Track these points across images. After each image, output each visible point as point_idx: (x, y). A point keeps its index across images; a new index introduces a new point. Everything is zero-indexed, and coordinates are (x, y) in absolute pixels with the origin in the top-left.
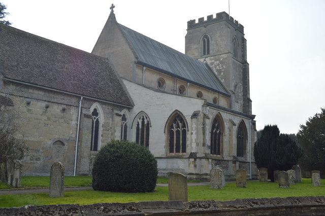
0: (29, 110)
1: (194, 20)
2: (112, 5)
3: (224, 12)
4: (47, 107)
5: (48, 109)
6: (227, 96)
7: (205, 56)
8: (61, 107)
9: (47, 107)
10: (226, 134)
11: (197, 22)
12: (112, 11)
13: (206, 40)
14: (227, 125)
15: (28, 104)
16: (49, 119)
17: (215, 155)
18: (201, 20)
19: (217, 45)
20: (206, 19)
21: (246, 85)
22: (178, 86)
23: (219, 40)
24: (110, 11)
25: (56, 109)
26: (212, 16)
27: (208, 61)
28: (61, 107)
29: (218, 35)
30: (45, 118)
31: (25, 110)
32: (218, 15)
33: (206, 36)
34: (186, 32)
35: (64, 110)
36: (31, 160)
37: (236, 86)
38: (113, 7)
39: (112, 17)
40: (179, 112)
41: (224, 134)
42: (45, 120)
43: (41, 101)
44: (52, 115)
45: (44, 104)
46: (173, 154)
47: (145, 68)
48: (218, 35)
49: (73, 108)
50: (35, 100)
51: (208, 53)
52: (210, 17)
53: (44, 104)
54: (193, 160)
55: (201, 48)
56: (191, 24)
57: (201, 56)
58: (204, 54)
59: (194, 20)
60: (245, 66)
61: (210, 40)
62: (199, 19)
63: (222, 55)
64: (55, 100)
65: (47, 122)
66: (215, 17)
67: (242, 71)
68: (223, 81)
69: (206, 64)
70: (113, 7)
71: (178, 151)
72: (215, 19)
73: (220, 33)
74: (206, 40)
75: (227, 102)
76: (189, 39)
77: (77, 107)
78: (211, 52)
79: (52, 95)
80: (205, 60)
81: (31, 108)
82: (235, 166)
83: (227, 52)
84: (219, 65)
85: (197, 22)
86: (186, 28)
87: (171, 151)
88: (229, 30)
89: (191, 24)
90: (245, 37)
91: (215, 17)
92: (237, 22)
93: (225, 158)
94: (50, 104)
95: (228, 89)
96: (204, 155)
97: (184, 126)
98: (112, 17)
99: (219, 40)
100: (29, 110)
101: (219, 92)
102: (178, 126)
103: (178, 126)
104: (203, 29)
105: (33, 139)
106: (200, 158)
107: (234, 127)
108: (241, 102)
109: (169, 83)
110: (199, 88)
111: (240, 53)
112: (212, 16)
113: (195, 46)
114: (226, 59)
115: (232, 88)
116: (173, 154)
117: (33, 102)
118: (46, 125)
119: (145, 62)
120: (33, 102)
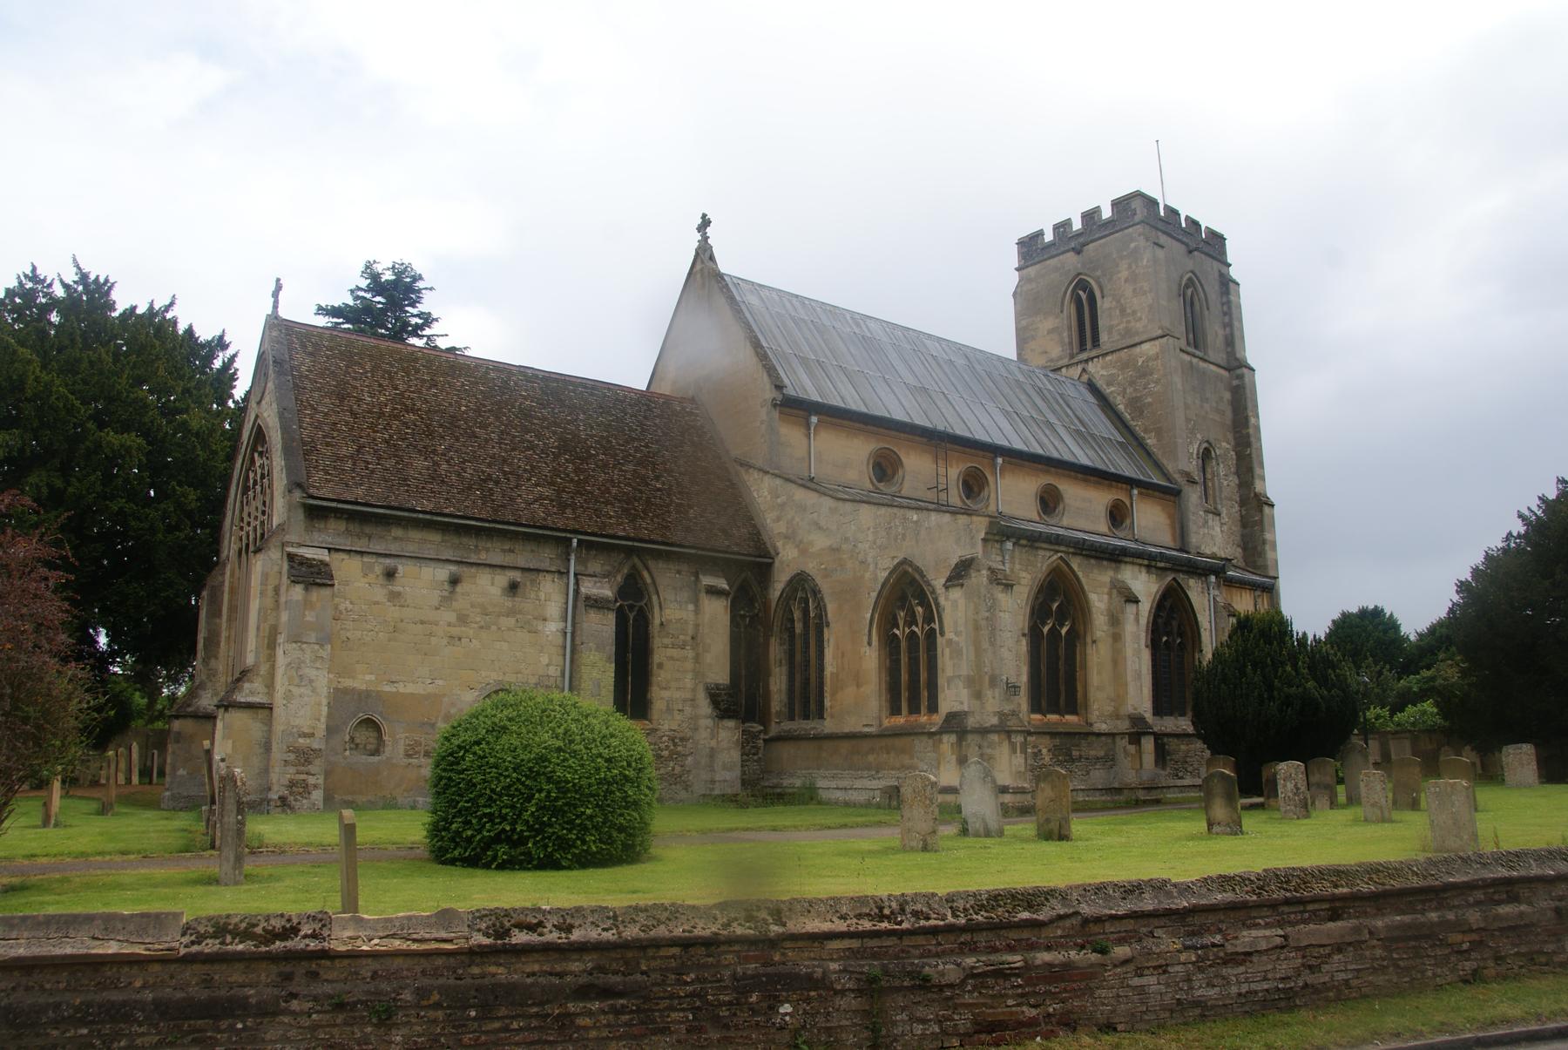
0: (394, 596)
1: (1040, 234)
2: (704, 216)
3: (1138, 195)
4: (454, 581)
5: (459, 589)
6: (1169, 494)
7: (1084, 356)
8: (502, 579)
9: (454, 581)
10: (1099, 634)
11: (1049, 237)
12: (705, 238)
13: (1083, 296)
14: (1099, 603)
15: (390, 574)
16: (463, 619)
17: (1053, 717)
20: (1077, 225)
21: (1249, 445)
22: (955, 472)
23: (1128, 290)
24: (698, 236)
25: (487, 587)
26: (1096, 211)
27: (1097, 370)
28: (502, 579)
29: (1124, 274)
30: (449, 616)
31: (379, 593)
32: (1116, 204)
33: (1083, 285)
34: (1014, 278)
35: (513, 587)
36: (409, 756)
37: (1206, 455)
38: (705, 223)
39: (704, 254)
40: (917, 569)
41: (1089, 640)
42: (449, 625)
43: (433, 564)
44: (472, 606)
45: (443, 573)
46: (900, 720)
47: (814, 419)
48: (1124, 274)
49: (549, 577)
50: (410, 562)
51: (1096, 342)
52: (1090, 216)
53: (443, 573)
54: (953, 738)
55: (1070, 328)
56: (1031, 248)
57: (1072, 356)
58: (1082, 347)
59: (1040, 234)
60: (1241, 377)
62: (1056, 228)
63: (1146, 346)
64: (483, 557)
65: (455, 631)
66: (1107, 213)
67: (1227, 396)
68: (1151, 441)
69: (1092, 387)
70: (705, 223)
71: (914, 709)
72: (1109, 222)
73: (1130, 267)
74: (1083, 296)
75: (1171, 516)
76: (1028, 303)
77: (559, 572)
78: (1104, 337)
79: (471, 542)
80: (1084, 370)
81: (401, 589)
82: (1140, 752)
83: (1160, 332)
85: (1049, 237)
86: (1014, 261)
87: (895, 710)
88: (1160, 253)
89: (1031, 248)
90: (1234, 273)
92: (1194, 224)
93: (1103, 727)
94: (465, 570)
95: (1170, 467)
96: (995, 721)
97: (929, 619)
98: (704, 254)
100: (394, 596)
101: (1131, 482)
102: (912, 621)
103: (912, 621)
105: (410, 689)
106: (984, 731)
107: (1131, 608)
108: (1230, 511)
109: (917, 466)
110: (1047, 472)
111: (1214, 332)
112: (1097, 210)
113: (1050, 323)
114: (1156, 357)
115: (1193, 466)
116: (900, 720)
117: (403, 568)
118: (454, 639)
119: (815, 397)
120: (403, 568)
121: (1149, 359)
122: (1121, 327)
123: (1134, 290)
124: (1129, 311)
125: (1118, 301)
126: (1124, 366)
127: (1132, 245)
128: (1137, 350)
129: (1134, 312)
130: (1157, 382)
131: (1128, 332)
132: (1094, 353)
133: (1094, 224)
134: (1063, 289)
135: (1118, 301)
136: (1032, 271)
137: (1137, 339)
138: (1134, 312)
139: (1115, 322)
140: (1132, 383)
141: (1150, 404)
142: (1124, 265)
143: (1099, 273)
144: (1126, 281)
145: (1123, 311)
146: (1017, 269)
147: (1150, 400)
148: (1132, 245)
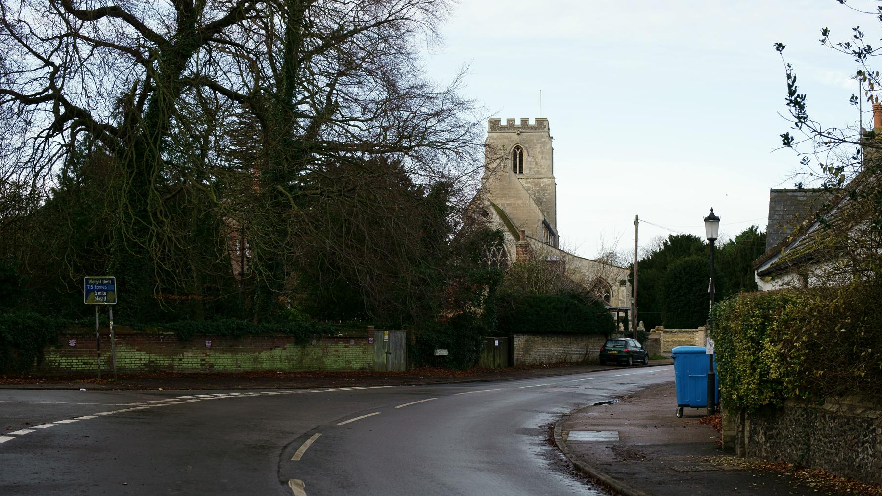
13: (518, 153)
18: (511, 122)
19: (536, 164)
20: (518, 123)
32: (537, 121)
33: (518, 148)
48: (538, 150)
51: (521, 172)
52: (525, 122)
59: (499, 121)
61: (525, 154)
63: (545, 180)
66: (532, 122)
72: (532, 128)
73: (541, 148)
84: (538, 192)
85: (504, 123)
91: (532, 122)
99: (540, 156)
104: (514, 136)
121: (546, 185)
122: (535, 169)
123: (542, 157)
124: (539, 164)
125: (535, 159)
126: (535, 185)
127: (543, 140)
128: (542, 180)
129: (541, 166)
130: (549, 194)
131: (538, 172)
132: (521, 176)
133: (527, 125)
134: (510, 147)
135: (535, 159)
136: (495, 135)
137: (541, 176)
138: (541, 166)
139: (533, 167)
140: (538, 192)
141: (545, 202)
142: (538, 146)
143: (527, 146)
144: (539, 152)
145: (536, 164)
146: (488, 132)
147: (545, 200)
148: (543, 140)
